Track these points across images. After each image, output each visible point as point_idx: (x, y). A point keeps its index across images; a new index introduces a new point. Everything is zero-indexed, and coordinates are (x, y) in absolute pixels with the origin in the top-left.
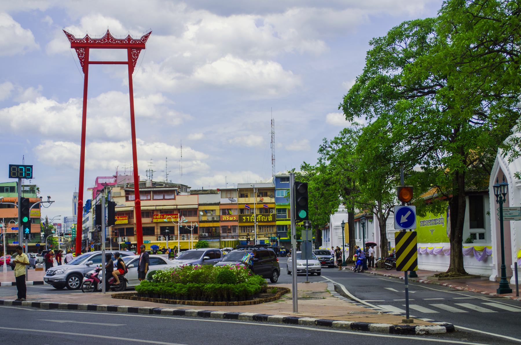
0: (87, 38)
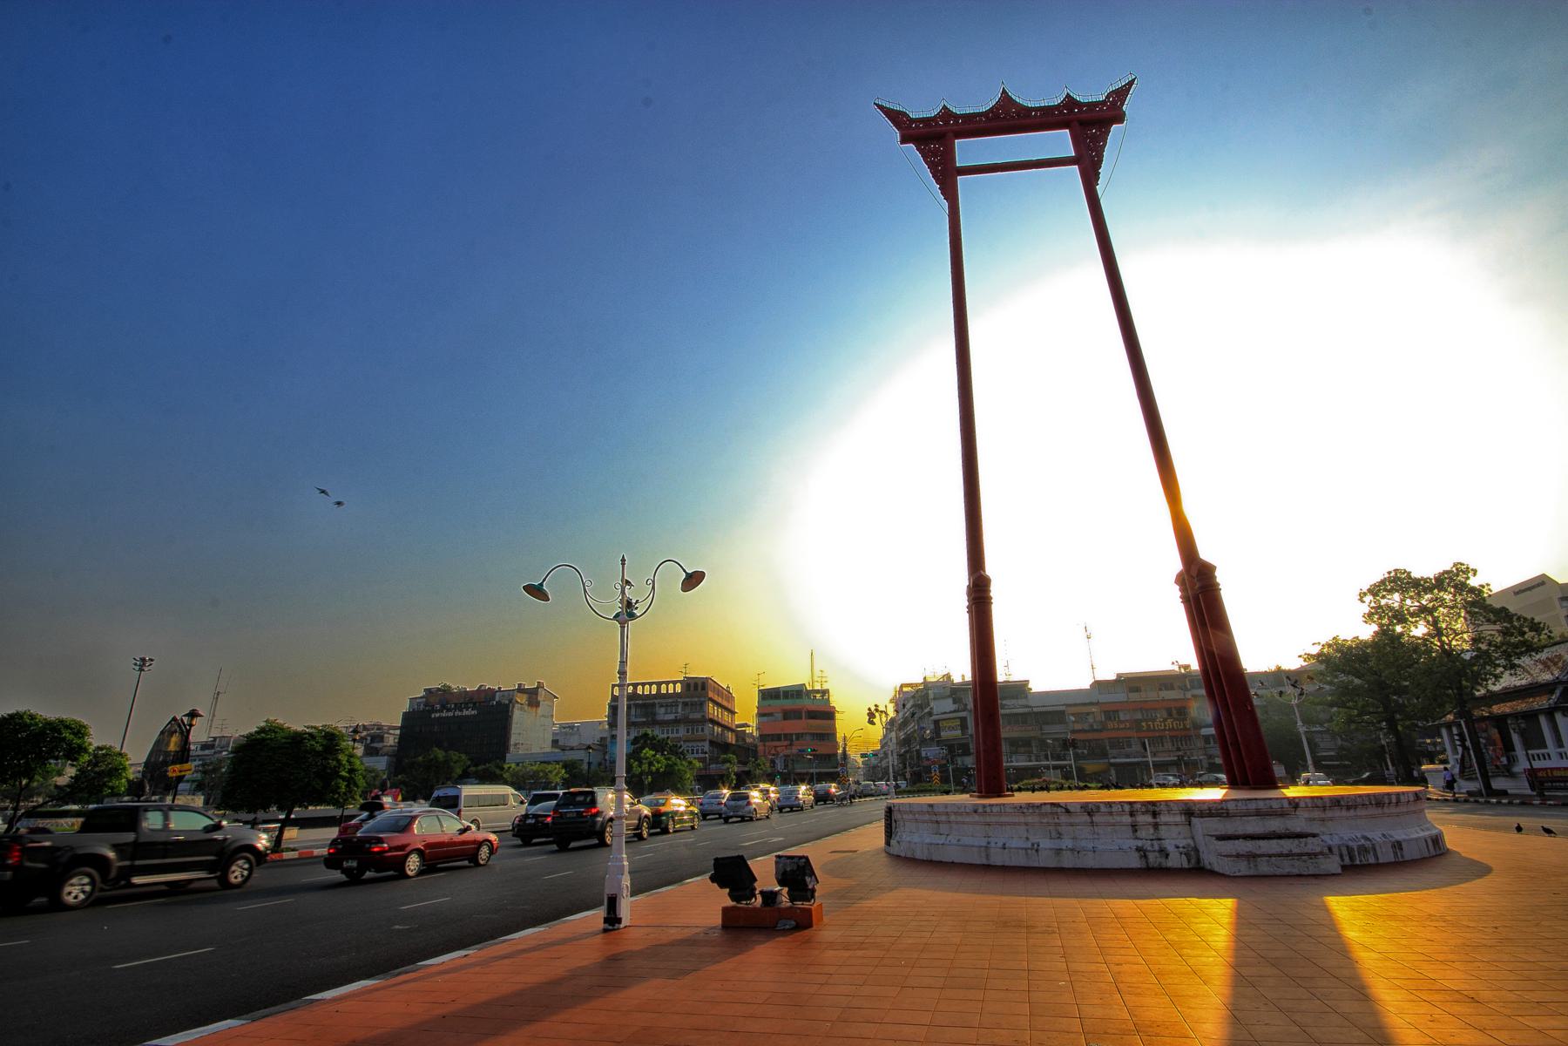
0: (946, 114)
